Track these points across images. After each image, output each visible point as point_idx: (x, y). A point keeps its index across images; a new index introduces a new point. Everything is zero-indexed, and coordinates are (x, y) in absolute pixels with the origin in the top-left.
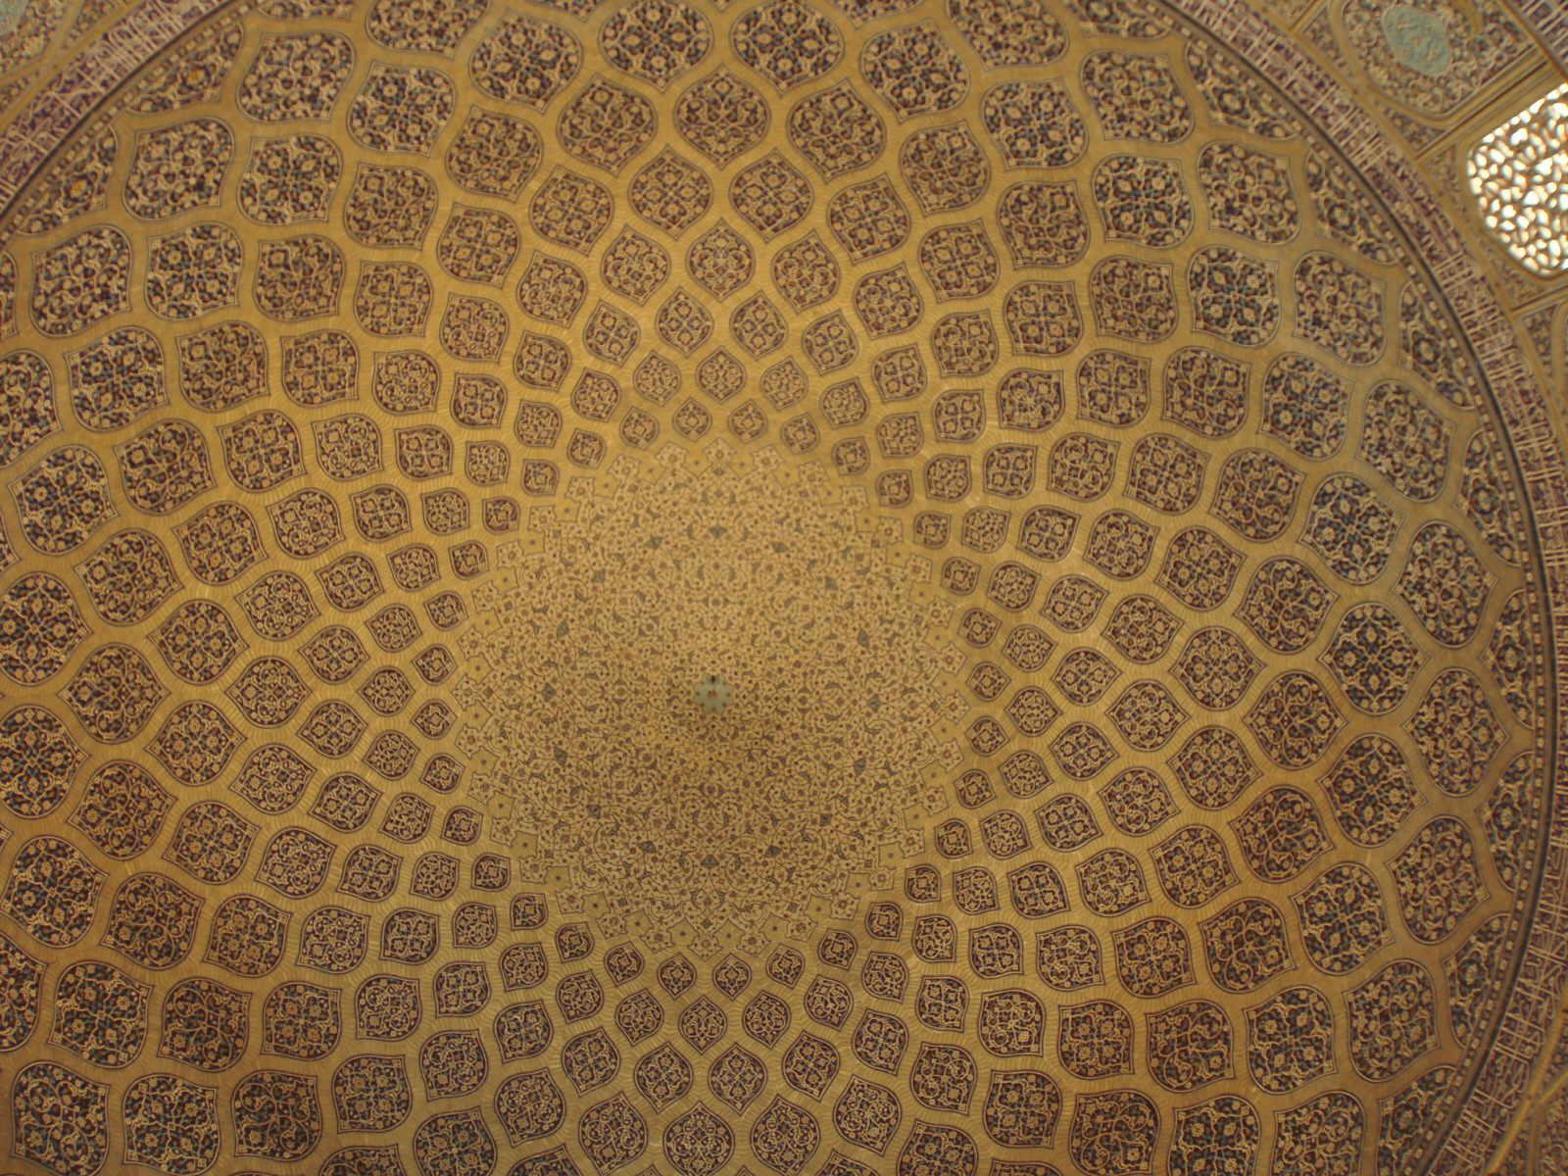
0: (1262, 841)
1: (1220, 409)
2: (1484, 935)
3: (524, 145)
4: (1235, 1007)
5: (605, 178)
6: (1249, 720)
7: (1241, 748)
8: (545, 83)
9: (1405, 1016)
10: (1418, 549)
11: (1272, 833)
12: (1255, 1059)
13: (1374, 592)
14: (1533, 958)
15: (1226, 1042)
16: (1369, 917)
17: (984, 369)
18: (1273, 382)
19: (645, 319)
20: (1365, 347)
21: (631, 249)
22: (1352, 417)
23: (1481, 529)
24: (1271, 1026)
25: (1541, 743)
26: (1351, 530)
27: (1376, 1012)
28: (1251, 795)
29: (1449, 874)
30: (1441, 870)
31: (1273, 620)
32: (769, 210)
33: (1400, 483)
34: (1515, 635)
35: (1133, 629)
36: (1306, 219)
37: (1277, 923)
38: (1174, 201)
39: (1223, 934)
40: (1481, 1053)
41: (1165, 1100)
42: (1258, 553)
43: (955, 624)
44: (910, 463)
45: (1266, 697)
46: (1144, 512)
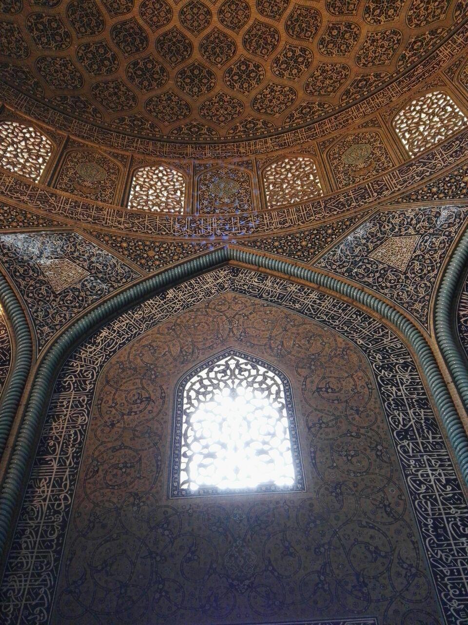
0: (170, 40)
2: (152, 126)
4: (105, 35)
6: (216, 30)
7: (205, 28)
9: (117, 101)
10: (287, 89)
11: (174, 44)
12: (87, 46)
13: (269, 74)
14: (148, 143)
15: (91, 34)
16: (150, 85)
18: (349, 26)
20: (363, 61)
23: (296, 111)
24: (102, 51)
25: (222, 138)
26: (292, 63)
27: (116, 90)
28: (188, 34)
29: (171, 112)
34: (259, 126)
36: (417, 31)
37: (141, 49)
39: (132, 28)
40: (111, 129)
42: (281, 27)
45: (225, 36)
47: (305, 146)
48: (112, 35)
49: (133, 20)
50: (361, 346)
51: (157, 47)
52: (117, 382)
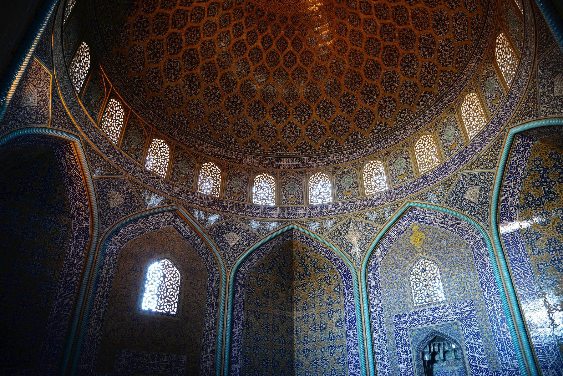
0: (191, 55)
1: (265, 94)
3: (403, 44)
4: (164, 38)
5: (386, 43)
7: (209, 58)
8: (405, 62)
10: (226, 118)
13: (223, 103)
16: (171, 77)
17: (301, 57)
18: (263, 108)
19: (362, 16)
20: (259, 132)
21: (373, 30)
22: (250, 119)
28: (200, 56)
30: (176, 98)
31: (228, 78)
32: (355, 55)
33: (237, 122)
34: (208, 133)
35: (240, 47)
38: (299, 118)
39: (178, 38)
41: (152, 16)
43: (264, 8)
44: (297, 27)
45: (215, 68)
46: (258, 65)
47: (221, 161)
48: (167, 38)
49: (180, 34)
50: (207, 269)
51: (183, 56)
52: (125, 258)
